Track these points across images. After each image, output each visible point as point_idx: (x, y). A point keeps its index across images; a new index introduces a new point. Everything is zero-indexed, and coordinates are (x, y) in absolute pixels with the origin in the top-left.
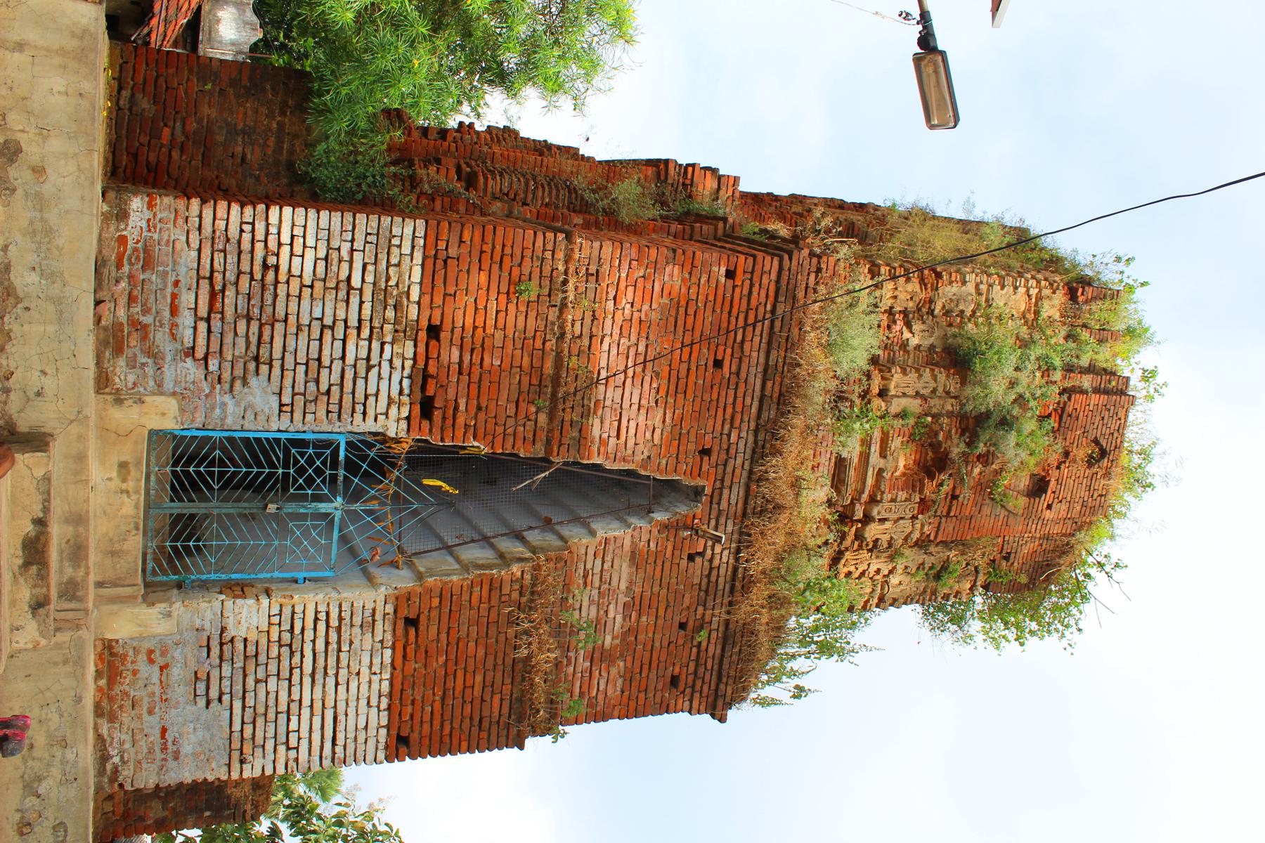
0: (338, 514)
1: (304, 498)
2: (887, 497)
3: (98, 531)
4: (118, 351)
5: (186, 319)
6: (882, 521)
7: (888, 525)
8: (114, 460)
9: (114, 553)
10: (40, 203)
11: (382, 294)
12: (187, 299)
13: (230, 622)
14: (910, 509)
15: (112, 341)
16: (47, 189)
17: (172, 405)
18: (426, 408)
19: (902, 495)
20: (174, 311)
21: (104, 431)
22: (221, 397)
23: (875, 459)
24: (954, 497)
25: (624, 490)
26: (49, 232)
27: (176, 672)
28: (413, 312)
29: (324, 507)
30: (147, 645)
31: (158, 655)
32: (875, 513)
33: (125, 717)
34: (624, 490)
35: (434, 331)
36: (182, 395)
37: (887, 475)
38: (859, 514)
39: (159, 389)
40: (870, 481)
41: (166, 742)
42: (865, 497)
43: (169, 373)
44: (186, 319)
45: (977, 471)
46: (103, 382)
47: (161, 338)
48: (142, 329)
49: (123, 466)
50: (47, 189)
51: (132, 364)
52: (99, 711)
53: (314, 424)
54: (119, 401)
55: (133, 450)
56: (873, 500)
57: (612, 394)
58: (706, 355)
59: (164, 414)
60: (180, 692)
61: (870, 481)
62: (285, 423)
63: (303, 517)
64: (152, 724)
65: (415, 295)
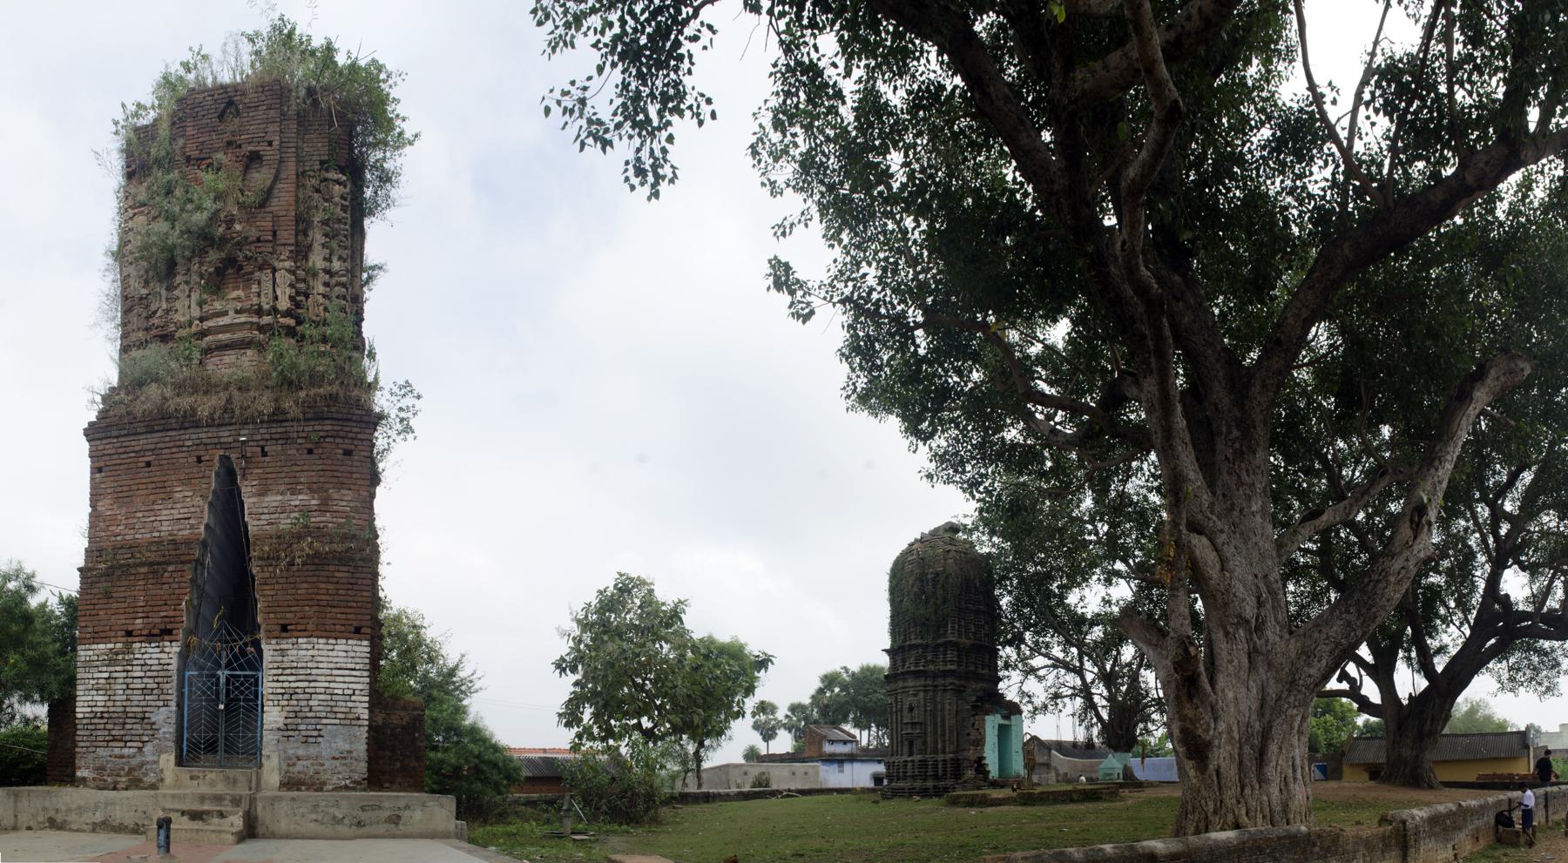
0: (227, 672)
1: (217, 691)
2: (255, 300)
3: (221, 789)
4: (140, 780)
5: (126, 751)
6: (276, 298)
7: (279, 292)
8: (189, 782)
9: (235, 781)
10: (69, 811)
11: (112, 662)
12: (117, 751)
13: (275, 726)
14: (266, 276)
15: (135, 783)
16: (63, 808)
17: (164, 757)
18: (169, 632)
19: (255, 288)
20: (122, 757)
21: (175, 787)
22: (160, 735)
23: (225, 320)
24: (258, 240)
25: (229, 506)
26: (79, 808)
27: (300, 752)
28: (119, 645)
29: (222, 680)
30: (284, 767)
31: (290, 761)
32: (266, 307)
33: (324, 777)
34: (229, 506)
35: (129, 634)
36: (160, 751)
37: (239, 306)
38: (266, 320)
39: (156, 762)
40: (243, 319)
41: (343, 757)
42: (255, 319)
43: (150, 758)
44: (126, 751)
45: (238, 227)
46: (153, 787)
47: (134, 762)
48: (131, 770)
49: (192, 778)
50: (63, 808)
51: (146, 775)
52: (321, 790)
53: (171, 688)
54: (162, 780)
55: (184, 773)
56: (259, 312)
57: (166, 527)
58: (144, 472)
59: (168, 760)
60: (313, 751)
61: (243, 319)
62: (173, 704)
63: (228, 691)
64: (328, 764)
65: (111, 646)
